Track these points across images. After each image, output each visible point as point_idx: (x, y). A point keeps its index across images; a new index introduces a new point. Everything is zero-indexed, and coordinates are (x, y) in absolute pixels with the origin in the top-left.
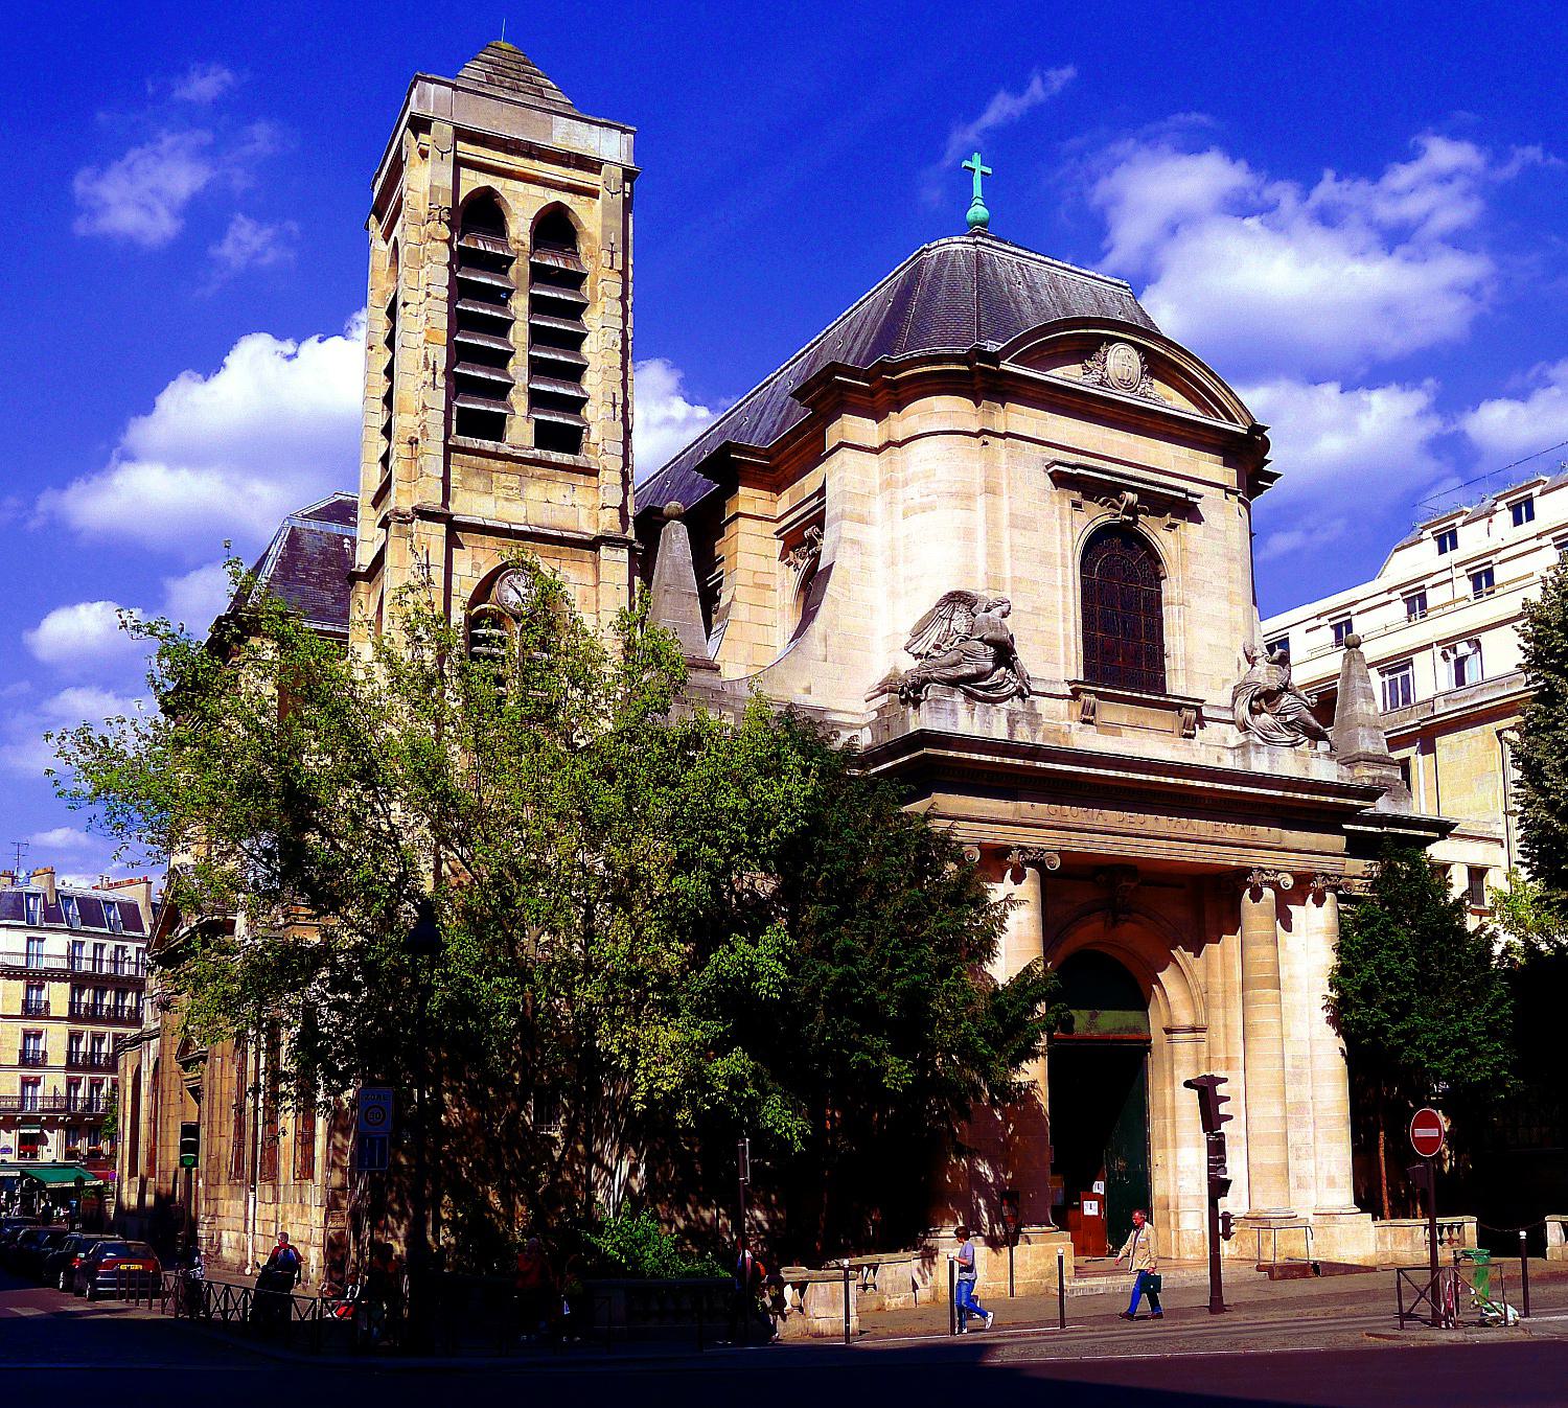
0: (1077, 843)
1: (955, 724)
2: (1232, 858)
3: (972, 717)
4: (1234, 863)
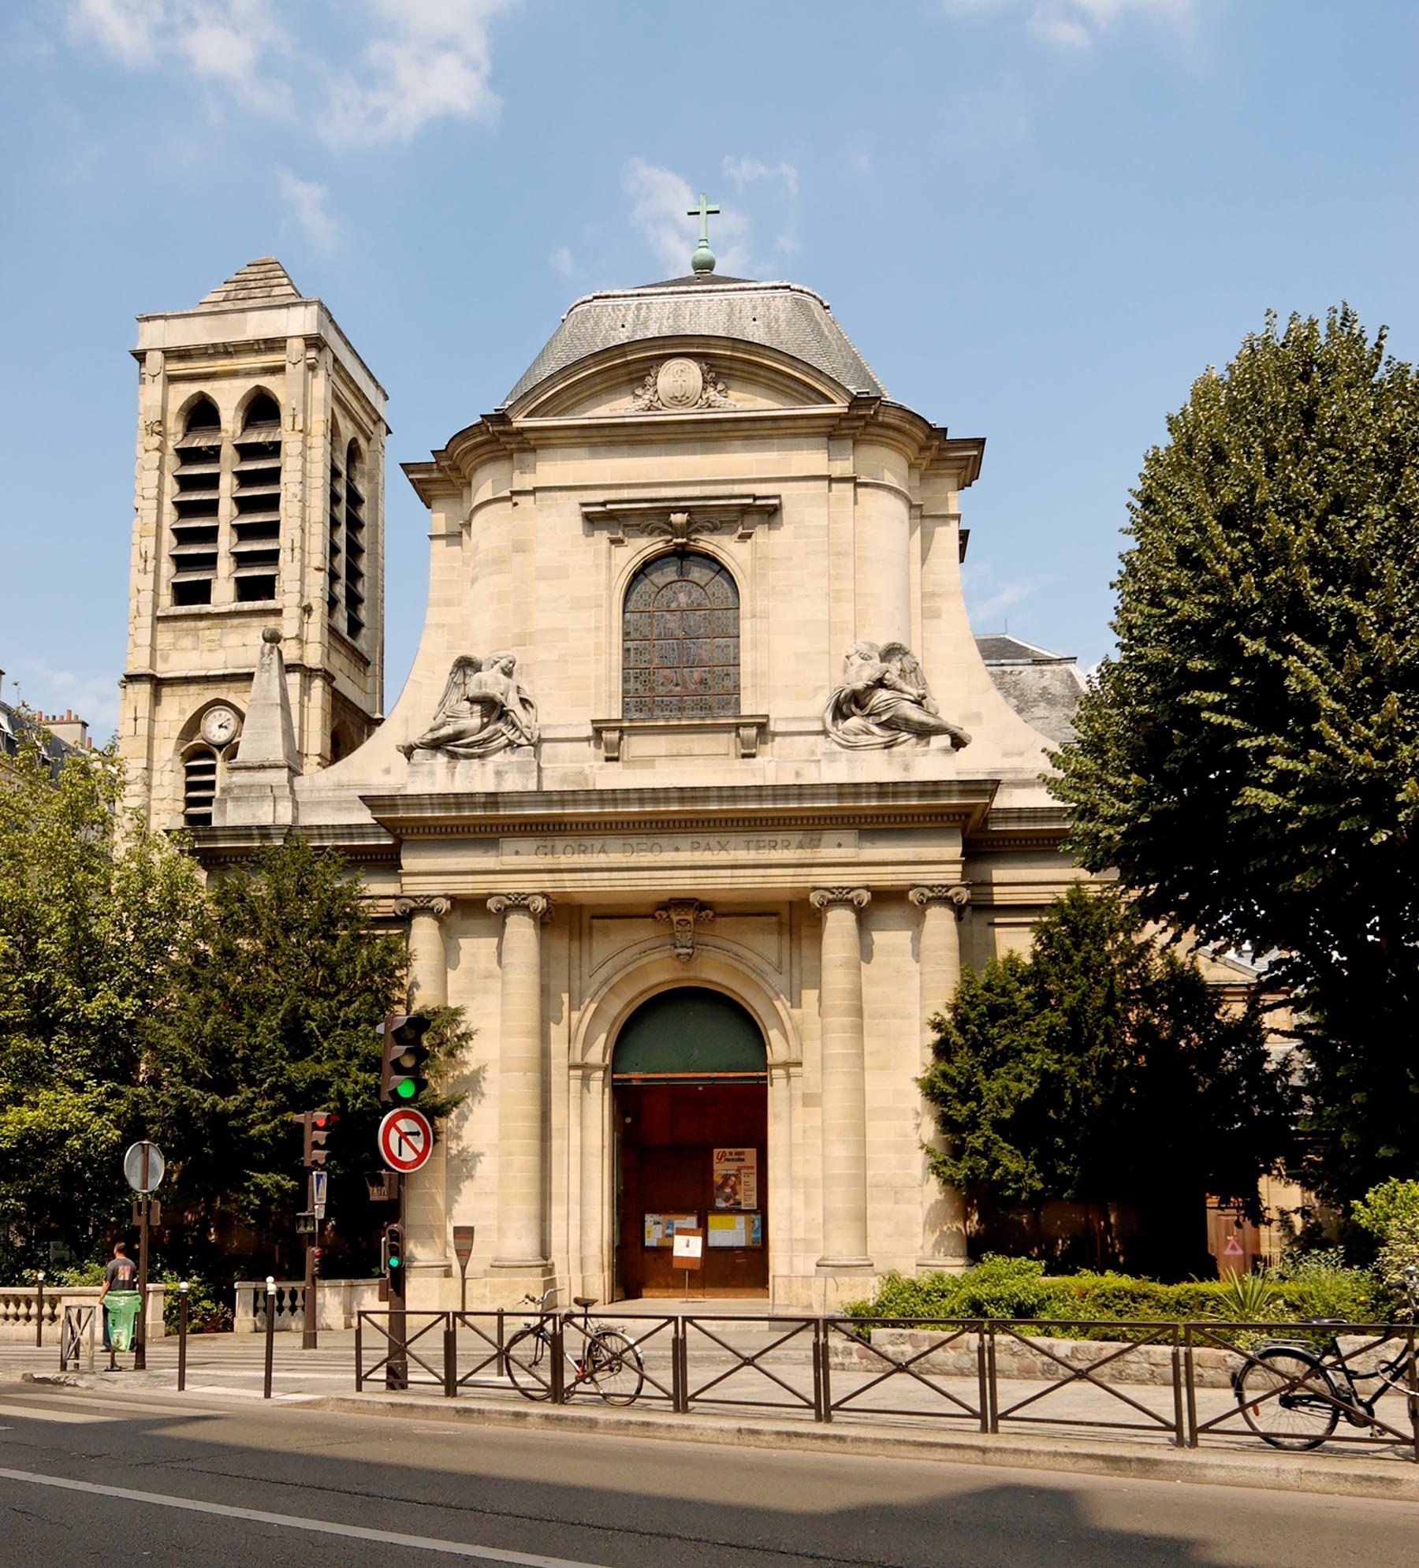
0: (569, 884)
1: (433, 784)
3: (453, 774)
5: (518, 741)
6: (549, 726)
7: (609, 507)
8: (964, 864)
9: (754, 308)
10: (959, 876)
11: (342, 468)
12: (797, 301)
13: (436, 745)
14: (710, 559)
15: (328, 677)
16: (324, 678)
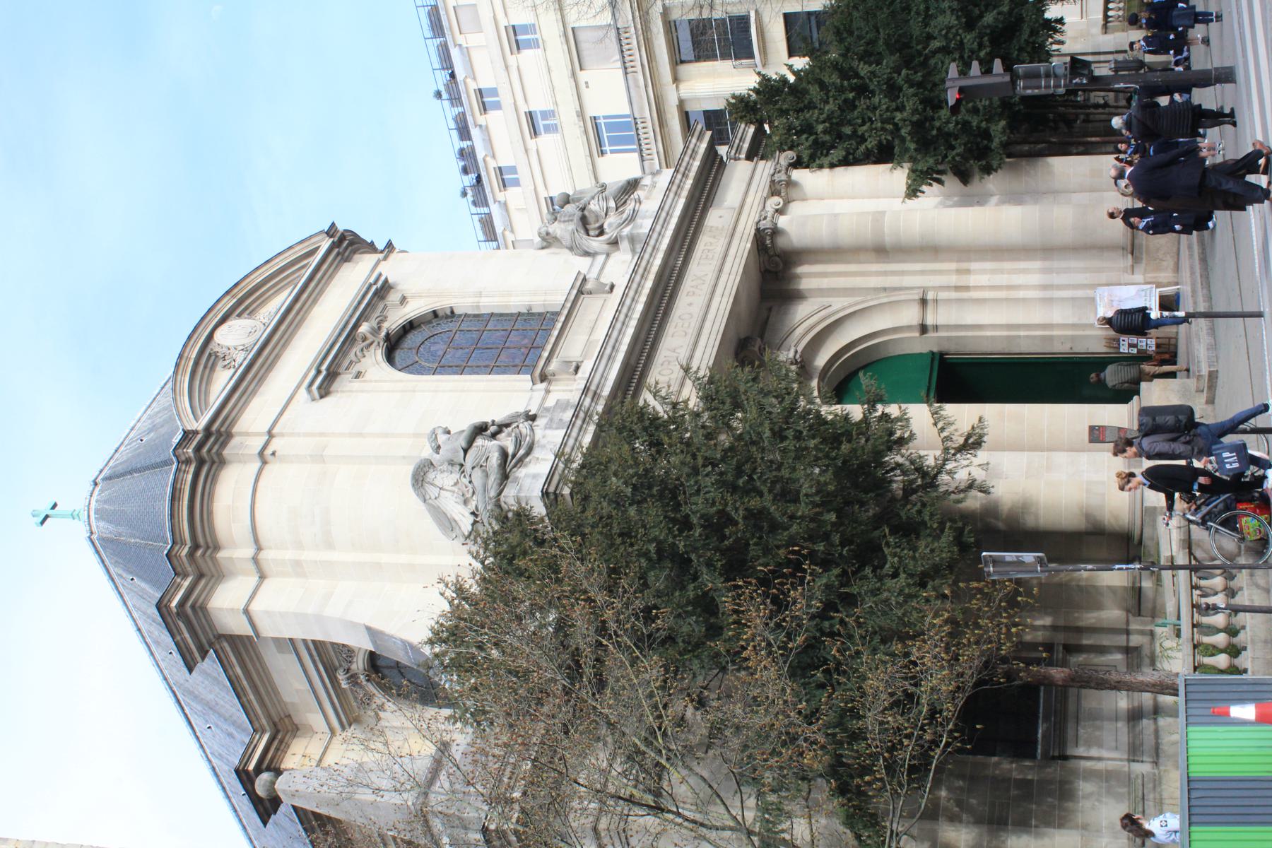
2: (743, 245)
4: (749, 245)
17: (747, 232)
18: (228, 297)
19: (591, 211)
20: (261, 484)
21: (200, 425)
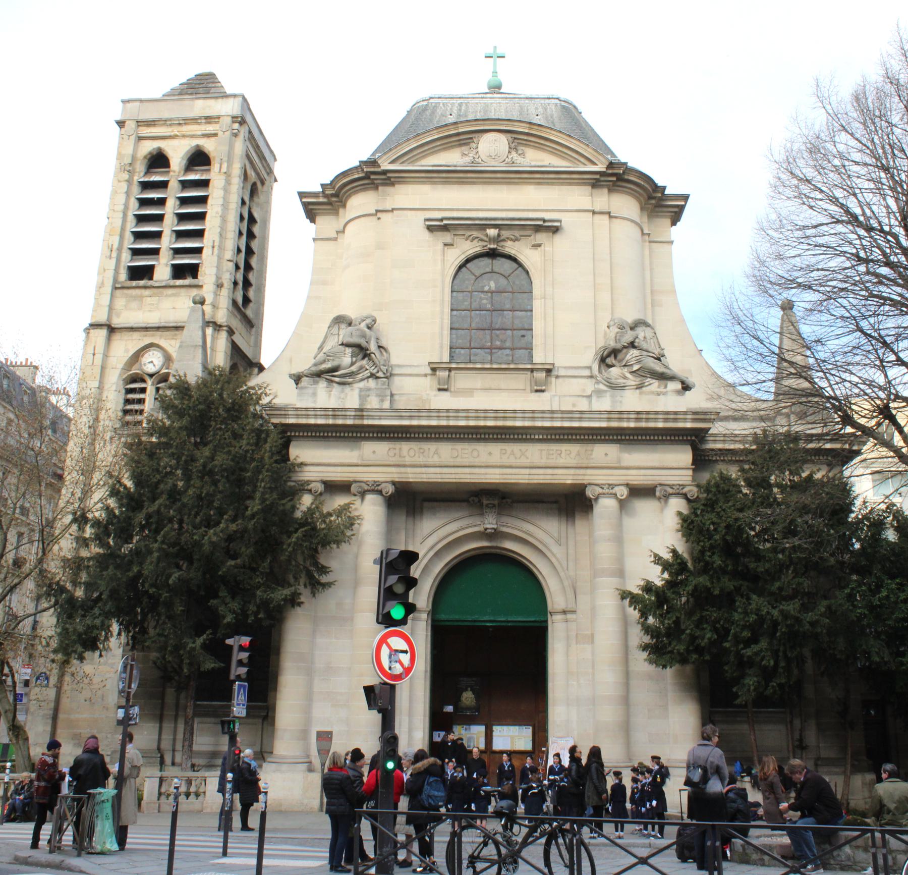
0: (412, 476)
1: (315, 402)
2: (567, 478)
4: (569, 482)
5: (378, 375)
6: (399, 366)
7: (445, 222)
8: (694, 470)
9: (536, 108)
10: (690, 478)
11: (247, 199)
12: (563, 107)
13: (318, 375)
14: (514, 259)
15: (231, 332)
16: (227, 331)
17: (587, 477)
18: (528, 125)
19: (626, 354)
20: (363, 219)
21: (385, 166)
